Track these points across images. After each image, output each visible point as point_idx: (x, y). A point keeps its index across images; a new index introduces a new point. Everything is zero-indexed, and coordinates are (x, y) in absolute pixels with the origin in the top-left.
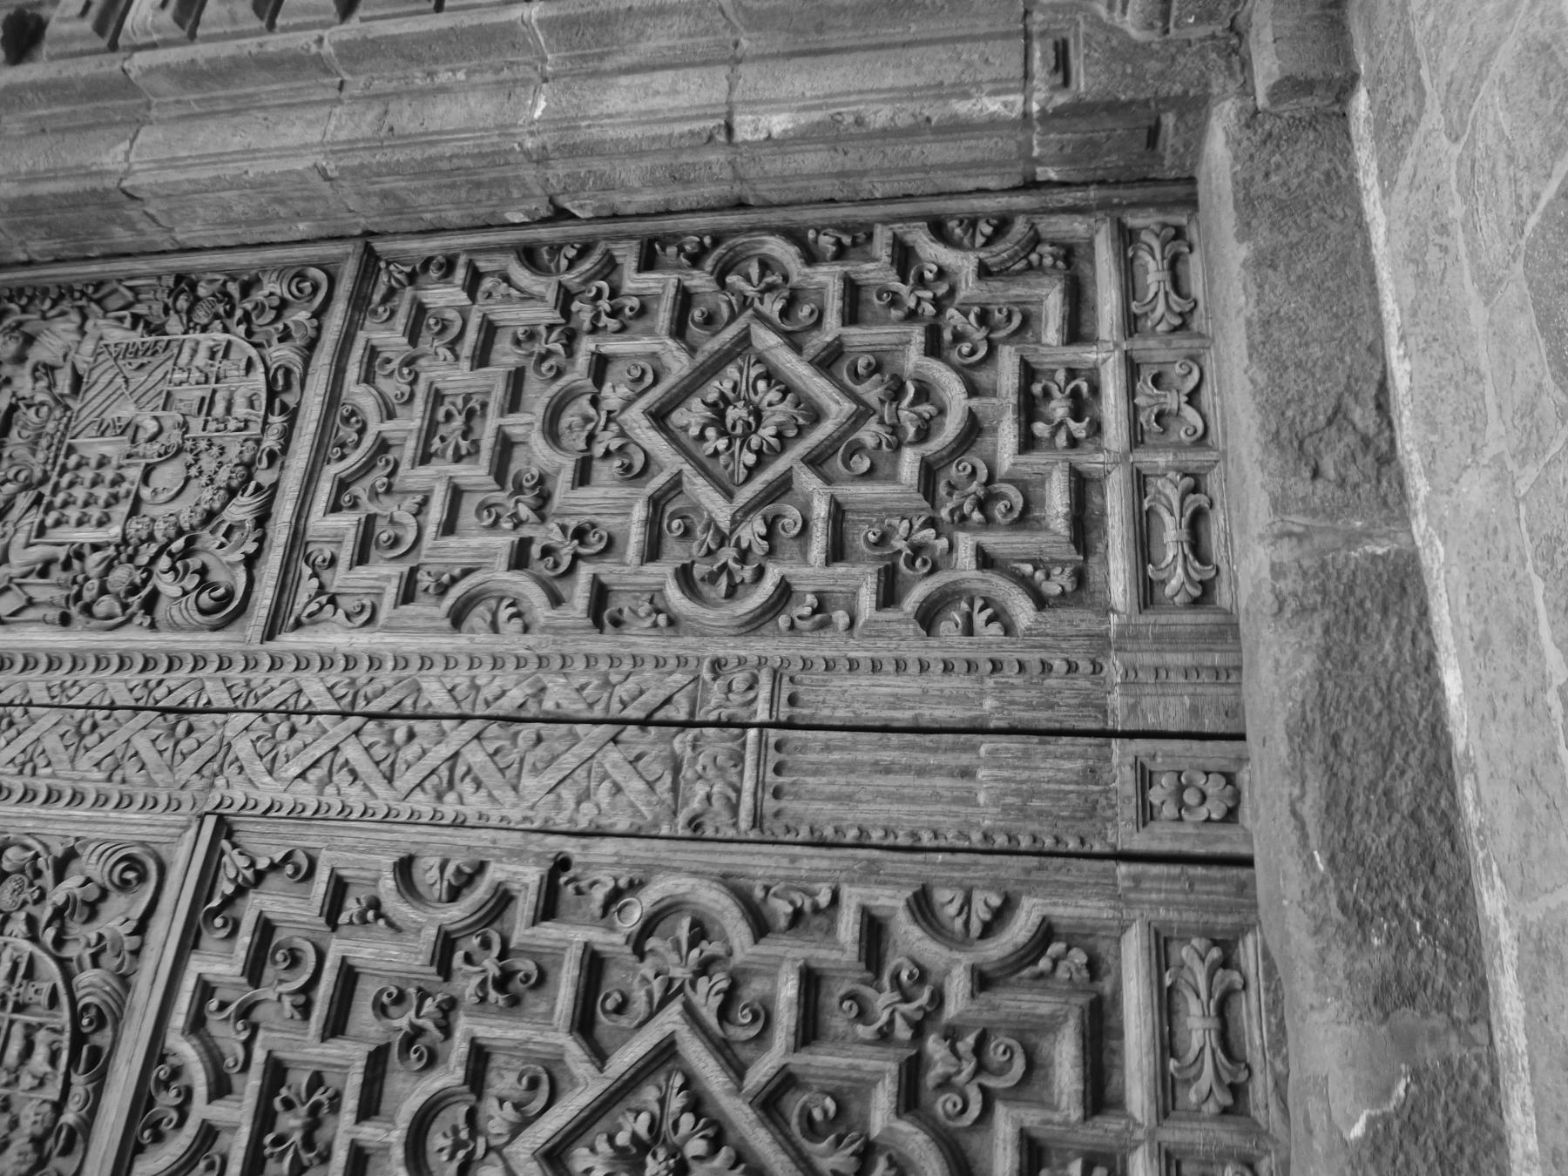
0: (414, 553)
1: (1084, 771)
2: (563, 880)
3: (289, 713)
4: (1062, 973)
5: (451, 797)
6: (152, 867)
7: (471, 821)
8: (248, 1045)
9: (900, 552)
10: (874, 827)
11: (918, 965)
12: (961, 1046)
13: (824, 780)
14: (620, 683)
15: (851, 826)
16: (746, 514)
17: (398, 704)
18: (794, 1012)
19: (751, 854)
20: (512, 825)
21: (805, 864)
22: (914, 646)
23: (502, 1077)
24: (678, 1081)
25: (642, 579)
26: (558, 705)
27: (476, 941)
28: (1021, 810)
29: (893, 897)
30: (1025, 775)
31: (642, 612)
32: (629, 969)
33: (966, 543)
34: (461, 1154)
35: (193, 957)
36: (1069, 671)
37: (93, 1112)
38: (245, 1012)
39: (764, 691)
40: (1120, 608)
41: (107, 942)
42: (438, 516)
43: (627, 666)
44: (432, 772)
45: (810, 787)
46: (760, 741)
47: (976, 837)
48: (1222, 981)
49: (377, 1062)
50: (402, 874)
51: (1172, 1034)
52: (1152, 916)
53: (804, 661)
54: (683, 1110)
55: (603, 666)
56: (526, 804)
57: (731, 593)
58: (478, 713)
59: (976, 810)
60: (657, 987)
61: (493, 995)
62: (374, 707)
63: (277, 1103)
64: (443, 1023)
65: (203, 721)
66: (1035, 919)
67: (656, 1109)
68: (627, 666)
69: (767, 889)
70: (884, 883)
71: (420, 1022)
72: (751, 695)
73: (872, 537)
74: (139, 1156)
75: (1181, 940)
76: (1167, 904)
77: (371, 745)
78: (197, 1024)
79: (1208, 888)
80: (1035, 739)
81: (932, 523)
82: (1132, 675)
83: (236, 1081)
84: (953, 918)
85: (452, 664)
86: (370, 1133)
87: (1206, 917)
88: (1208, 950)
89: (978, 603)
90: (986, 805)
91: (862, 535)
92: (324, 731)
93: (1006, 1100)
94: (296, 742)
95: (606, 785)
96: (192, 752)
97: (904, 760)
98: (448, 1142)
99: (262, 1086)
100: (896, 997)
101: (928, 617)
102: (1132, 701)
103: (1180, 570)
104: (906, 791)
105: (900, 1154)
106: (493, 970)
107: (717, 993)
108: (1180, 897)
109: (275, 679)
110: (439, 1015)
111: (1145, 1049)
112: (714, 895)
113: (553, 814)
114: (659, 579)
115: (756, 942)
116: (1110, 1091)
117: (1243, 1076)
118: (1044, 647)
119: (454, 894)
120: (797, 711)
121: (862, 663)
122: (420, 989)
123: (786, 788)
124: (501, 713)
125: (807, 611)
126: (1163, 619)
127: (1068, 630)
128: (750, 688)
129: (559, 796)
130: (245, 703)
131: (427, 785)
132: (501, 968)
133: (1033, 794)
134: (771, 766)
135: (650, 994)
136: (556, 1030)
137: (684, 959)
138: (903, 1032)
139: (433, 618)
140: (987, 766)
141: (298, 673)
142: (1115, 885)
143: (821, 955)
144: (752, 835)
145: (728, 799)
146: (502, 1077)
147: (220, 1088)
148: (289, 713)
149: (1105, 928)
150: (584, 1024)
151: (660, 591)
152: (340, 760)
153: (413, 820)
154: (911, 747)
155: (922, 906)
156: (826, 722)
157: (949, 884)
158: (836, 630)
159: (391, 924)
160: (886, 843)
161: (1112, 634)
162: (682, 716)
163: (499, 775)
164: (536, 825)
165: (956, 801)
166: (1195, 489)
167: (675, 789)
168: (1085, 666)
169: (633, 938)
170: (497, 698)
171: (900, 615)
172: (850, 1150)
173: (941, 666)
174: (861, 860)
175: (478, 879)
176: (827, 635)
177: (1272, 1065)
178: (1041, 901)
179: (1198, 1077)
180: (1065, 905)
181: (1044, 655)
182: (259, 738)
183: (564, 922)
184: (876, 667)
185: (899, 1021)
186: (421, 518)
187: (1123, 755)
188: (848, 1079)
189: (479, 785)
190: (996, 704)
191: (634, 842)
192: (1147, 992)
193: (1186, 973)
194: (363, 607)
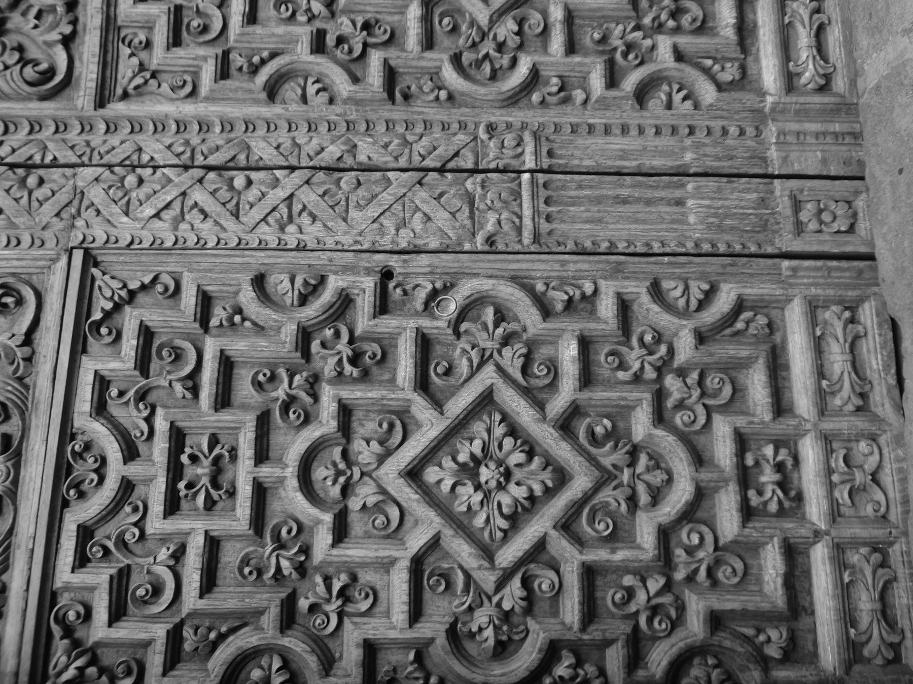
0: (223, 38)
4: (752, 330)
5: (291, 229)
6: (29, 295)
7: (310, 245)
8: (149, 420)
9: (615, 49)
10: (620, 240)
11: (656, 331)
12: (688, 381)
13: (582, 208)
14: (416, 142)
15: (604, 240)
16: (500, 16)
17: (233, 158)
18: (577, 366)
19: (533, 261)
20: (346, 247)
21: (572, 267)
22: (632, 116)
23: (363, 425)
24: (498, 417)
25: (423, 64)
26: (369, 158)
27: (329, 333)
28: (719, 227)
29: (638, 286)
30: (721, 203)
31: (426, 89)
32: (449, 345)
33: (665, 44)
34: (342, 480)
35: (84, 358)
36: (740, 135)
37: (16, 482)
38: (142, 396)
39: (529, 148)
40: (772, 91)
42: (241, 8)
43: (419, 129)
44: (274, 209)
45: (571, 214)
46: (533, 182)
47: (690, 246)
48: (851, 332)
49: (263, 422)
50: (258, 286)
51: (822, 365)
52: (807, 292)
53: (556, 125)
54: (505, 435)
55: (400, 129)
56: (355, 231)
57: (494, 77)
58: (303, 164)
60: (475, 355)
61: (348, 368)
62: (213, 160)
63: (184, 459)
64: (311, 392)
65: (55, 174)
66: (733, 296)
68: (419, 129)
69: (547, 285)
70: (628, 278)
71: (294, 392)
72: (520, 150)
73: (597, 36)
74: (65, 510)
75: (823, 307)
76: (816, 285)
77: (216, 191)
78: (100, 409)
79: (838, 274)
80: (725, 179)
81: (637, 28)
82: (782, 137)
83: (142, 448)
84: (677, 299)
85: (272, 127)
88: (842, 312)
89: (676, 87)
90: (695, 224)
91: (589, 36)
92: (170, 181)
93: (717, 412)
94: (146, 189)
95: (418, 215)
96: (47, 199)
97: (636, 195)
98: (331, 472)
100: (644, 351)
101: (641, 95)
102: (784, 154)
103: (811, 66)
104: (639, 216)
105: (654, 451)
106: (347, 352)
107: (519, 357)
108: (821, 281)
109: (114, 140)
110: (308, 386)
111: (808, 375)
113: (378, 238)
114: (438, 64)
116: (784, 404)
117: (867, 388)
118: (721, 117)
119: (303, 300)
120: (555, 161)
121: (598, 128)
122: (288, 370)
123: (555, 215)
124: (323, 164)
125: (555, 89)
126: (802, 100)
127: (737, 106)
128: (518, 145)
129: (382, 225)
130: (90, 159)
131: (270, 219)
132: (353, 350)
133: (726, 216)
134: (542, 200)
135: (470, 360)
136: (403, 390)
137: (491, 337)
138: (650, 373)
139: (251, 91)
140: (693, 197)
141: (133, 136)
142: (780, 274)
143: (591, 327)
144: (533, 249)
145: (514, 223)
146: (363, 425)
147: (130, 453)
148: (134, 167)
149: (777, 301)
150: (423, 384)
151: (437, 73)
152: (189, 202)
153: (262, 246)
154: (640, 185)
155: (656, 292)
156: (576, 170)
157: (672, 277)
158: (574, 104)
159: (255, 324)
160: (627, 251)
161: (767, 110)
162: (470, 165)
163: (332, 211)
164: (366, 246)
165: (673, 221)
166: (818, 11)
167: (472, 217)
168: (750, 131)
169: (453, 323)
170: (318, 153)
171: (623, 94)
172: (624, 451)
173: (654, 130)
174: (611, 263)
175: (320, 288)
176: (568, 108)
178: (735, 285)
180: (752, 287)
181: (725, 123)
183: (395, 315)
184: (607, 131)
185: (647, 367)
186: (224, 10)
187: (783, 190)
188: (617, 406)
189: (314, 218)
190: (694, 156)
191: (443, 256)
192: (807, 340)
193: (829, 327)
194: (185, 82)
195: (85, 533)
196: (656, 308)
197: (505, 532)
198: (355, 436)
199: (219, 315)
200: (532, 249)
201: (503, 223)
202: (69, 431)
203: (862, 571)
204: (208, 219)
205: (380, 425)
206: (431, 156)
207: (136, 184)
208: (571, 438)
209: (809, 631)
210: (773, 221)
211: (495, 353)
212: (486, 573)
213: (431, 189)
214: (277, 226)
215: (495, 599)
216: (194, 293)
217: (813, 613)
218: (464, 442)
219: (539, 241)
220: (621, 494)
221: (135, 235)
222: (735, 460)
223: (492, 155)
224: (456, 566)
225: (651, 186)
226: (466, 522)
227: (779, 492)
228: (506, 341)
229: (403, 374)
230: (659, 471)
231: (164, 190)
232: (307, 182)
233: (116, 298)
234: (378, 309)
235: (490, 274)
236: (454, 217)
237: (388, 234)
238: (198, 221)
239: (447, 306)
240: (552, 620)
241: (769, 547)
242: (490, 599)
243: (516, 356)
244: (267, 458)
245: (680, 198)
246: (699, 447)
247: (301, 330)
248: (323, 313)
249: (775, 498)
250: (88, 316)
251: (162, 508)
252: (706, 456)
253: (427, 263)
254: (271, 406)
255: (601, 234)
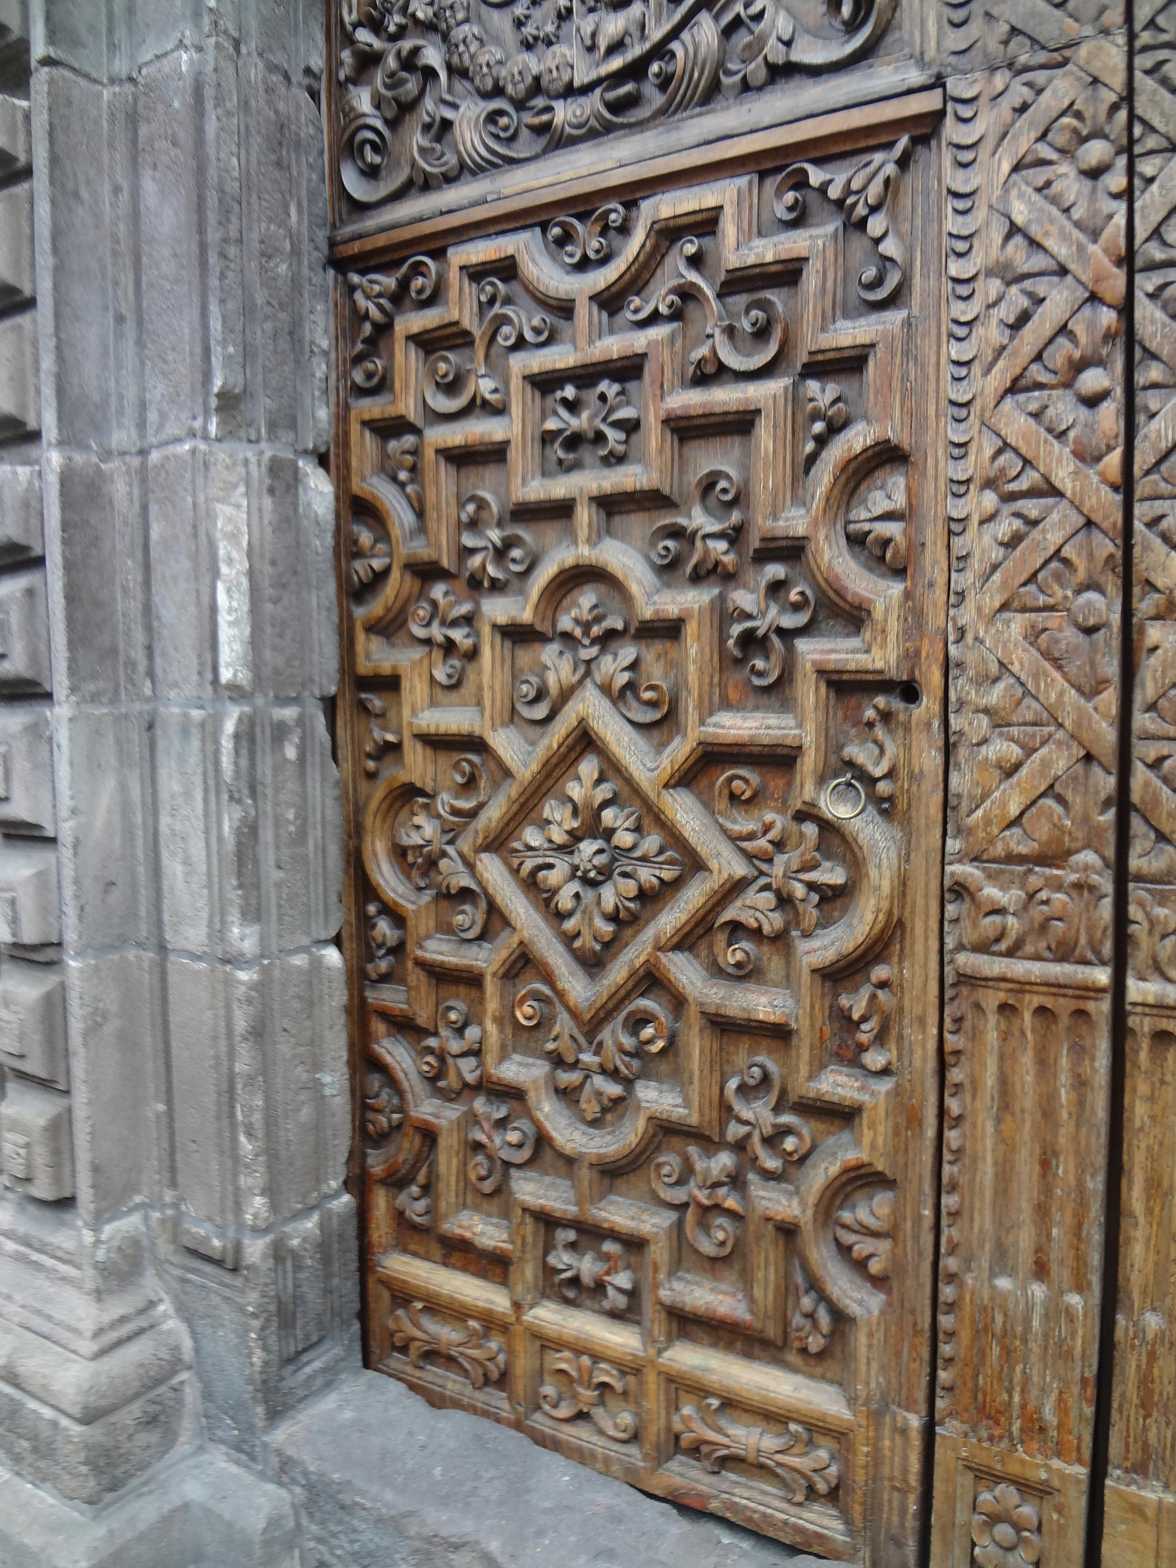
1: (1040, 1419)
2: (881, 701)
3: (1128, 148)
5: (990, 500)
8: (654, 318)
10: (963, 1136)
12: (722, 1191)
20: (952, 612)
24: (668, 874)
26: (1156, 648)
27: (794, 596)
29: (873, 1146)
30: (1035, 1346)
32: (785, 802)
34: (578, 632)
37: (573, 141)
38: (687, 294)
41: (759, 28)
44: (1027, 462)
46: (1087, 989)
47: (950, 1263)
48: (794, 1481)
51: (746, 1411)
58: (1138, 509)
59: (986, 1274)
60: (762, 843)
61: (736, 629)
63: (604, 386)
64: (703, 572)
66: (854, 1309)
67: (637, 853)
69: (883, 985)
70: (896, 1133)
77: (1072, 336)
79: (895, 1504)
80: (1091, 1372)
86: (584, 514)
87: (859, 1492)
90: (993, 1288)
92: (1095, 235)
95: (1016, 752)
98: (586, 616)
99: (611, 361)
100: (768, 1131)
106: (761, 625)
110: (710, 566)
111: (725, 1382)
112: (869, 917)
113: (971, 673)
115: (814, 971)
116: (693, 1329)
119: (856, 541)
120: (1145, 1044)
123: (1016, 1022)
124: (1137, 551)
129: (996, 680)
130: (1146, 49)
132: (765, 636)
134: (1048, 1002)
136: (702, 723)
138: (735, 1131)
143: (804, 1049)
145: (998, 940)
146: (659, 657)
148: (1128, 148)
152: (1040, 287)
159: (812, 459)
162: (1135, 863)
164: (953, 650)
167: (1011, 858)
172: (619, 1063)
175: (883, 568)
177: (716, 1497)
179: (703, 1419)
180: (870, 1346)
182: (1079, 115)
187: (1063, 1476)
191: (938, 797)
195: (507, 269)
196: (835, 1169)
197: (518, 871)
198: (644, 648)
199: (821, 393)
200: (947, 969)
201: (997, 919)
202: (638, 195)
203: (478, 1346)
204: (1007, 332)
205: (652, 688)
206: (1158, 783)
207: (1085, 166)
208: (635, 987)
209: (427, 1252)
210: (996, 1432)
211: (767, 880)
212: (470, 840)
213: (1075, 779)
214: (992, 474)
215: (450, 850)
216: (859, 341)
217: (445, 1265)
218: (632, 819)
219: (964, 983)
220: (565, 1046)
221: (976, 198)
222: (606, 1225)
223: (1161, 912)
224: (481, 799)
225: (1080, 1226)
226: (533, 815)
227: (568, 1274)
228: (784, 901)
229: (728, 724)
230: (597, 1109)
231: (1069, 226)
232: (1089, 524)
233: (849, 201)
234: (835, 677)
235: (909, 883)
236: (1011, 824)
237: (977, 692)
238: (1002, 315)
239: (845, 801)
240: (432, 924)
241: (505, 1236)
242: (451, 842)
243: (758, 915)
244: (609, 515)
245: (1048, 1273)
246: (632, 1177)
247: (797, 543)
248: (826, 580)
249: (561, 1267)
250: (817, 162)
251: (536, 370)
252: (620, 1183)
253: (925, 769)
254: (683, 508)
255: (978, 1103)
